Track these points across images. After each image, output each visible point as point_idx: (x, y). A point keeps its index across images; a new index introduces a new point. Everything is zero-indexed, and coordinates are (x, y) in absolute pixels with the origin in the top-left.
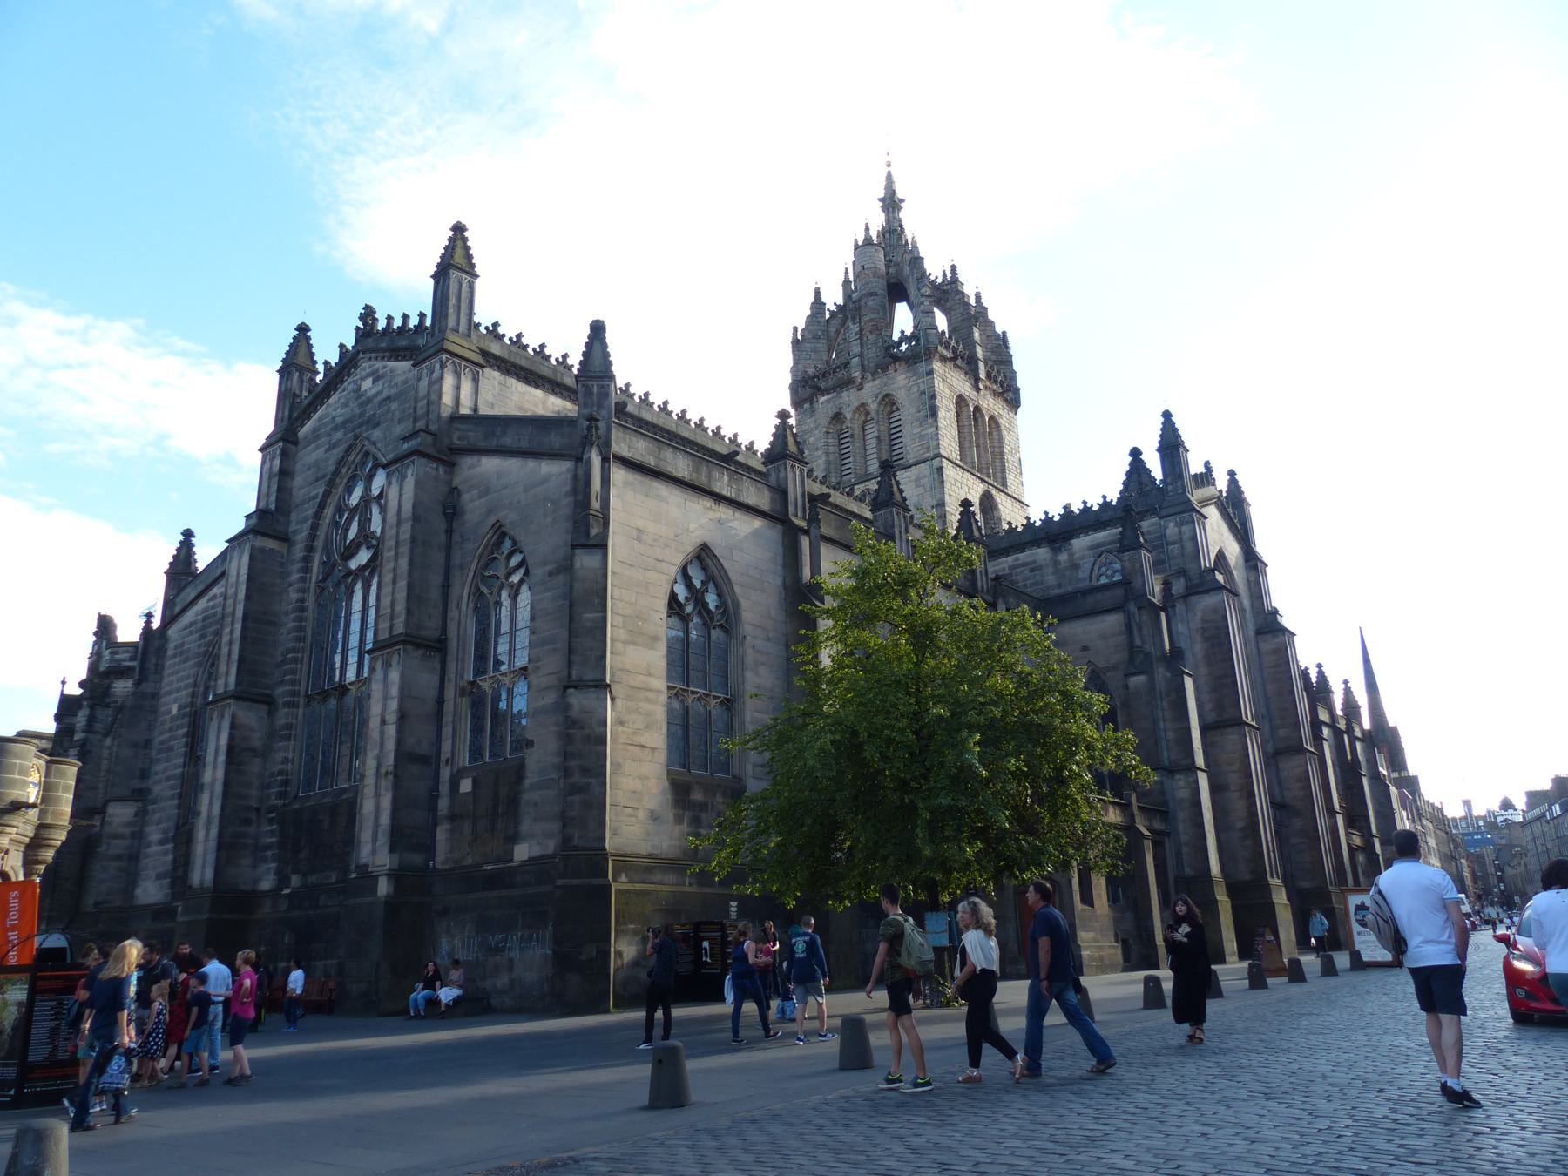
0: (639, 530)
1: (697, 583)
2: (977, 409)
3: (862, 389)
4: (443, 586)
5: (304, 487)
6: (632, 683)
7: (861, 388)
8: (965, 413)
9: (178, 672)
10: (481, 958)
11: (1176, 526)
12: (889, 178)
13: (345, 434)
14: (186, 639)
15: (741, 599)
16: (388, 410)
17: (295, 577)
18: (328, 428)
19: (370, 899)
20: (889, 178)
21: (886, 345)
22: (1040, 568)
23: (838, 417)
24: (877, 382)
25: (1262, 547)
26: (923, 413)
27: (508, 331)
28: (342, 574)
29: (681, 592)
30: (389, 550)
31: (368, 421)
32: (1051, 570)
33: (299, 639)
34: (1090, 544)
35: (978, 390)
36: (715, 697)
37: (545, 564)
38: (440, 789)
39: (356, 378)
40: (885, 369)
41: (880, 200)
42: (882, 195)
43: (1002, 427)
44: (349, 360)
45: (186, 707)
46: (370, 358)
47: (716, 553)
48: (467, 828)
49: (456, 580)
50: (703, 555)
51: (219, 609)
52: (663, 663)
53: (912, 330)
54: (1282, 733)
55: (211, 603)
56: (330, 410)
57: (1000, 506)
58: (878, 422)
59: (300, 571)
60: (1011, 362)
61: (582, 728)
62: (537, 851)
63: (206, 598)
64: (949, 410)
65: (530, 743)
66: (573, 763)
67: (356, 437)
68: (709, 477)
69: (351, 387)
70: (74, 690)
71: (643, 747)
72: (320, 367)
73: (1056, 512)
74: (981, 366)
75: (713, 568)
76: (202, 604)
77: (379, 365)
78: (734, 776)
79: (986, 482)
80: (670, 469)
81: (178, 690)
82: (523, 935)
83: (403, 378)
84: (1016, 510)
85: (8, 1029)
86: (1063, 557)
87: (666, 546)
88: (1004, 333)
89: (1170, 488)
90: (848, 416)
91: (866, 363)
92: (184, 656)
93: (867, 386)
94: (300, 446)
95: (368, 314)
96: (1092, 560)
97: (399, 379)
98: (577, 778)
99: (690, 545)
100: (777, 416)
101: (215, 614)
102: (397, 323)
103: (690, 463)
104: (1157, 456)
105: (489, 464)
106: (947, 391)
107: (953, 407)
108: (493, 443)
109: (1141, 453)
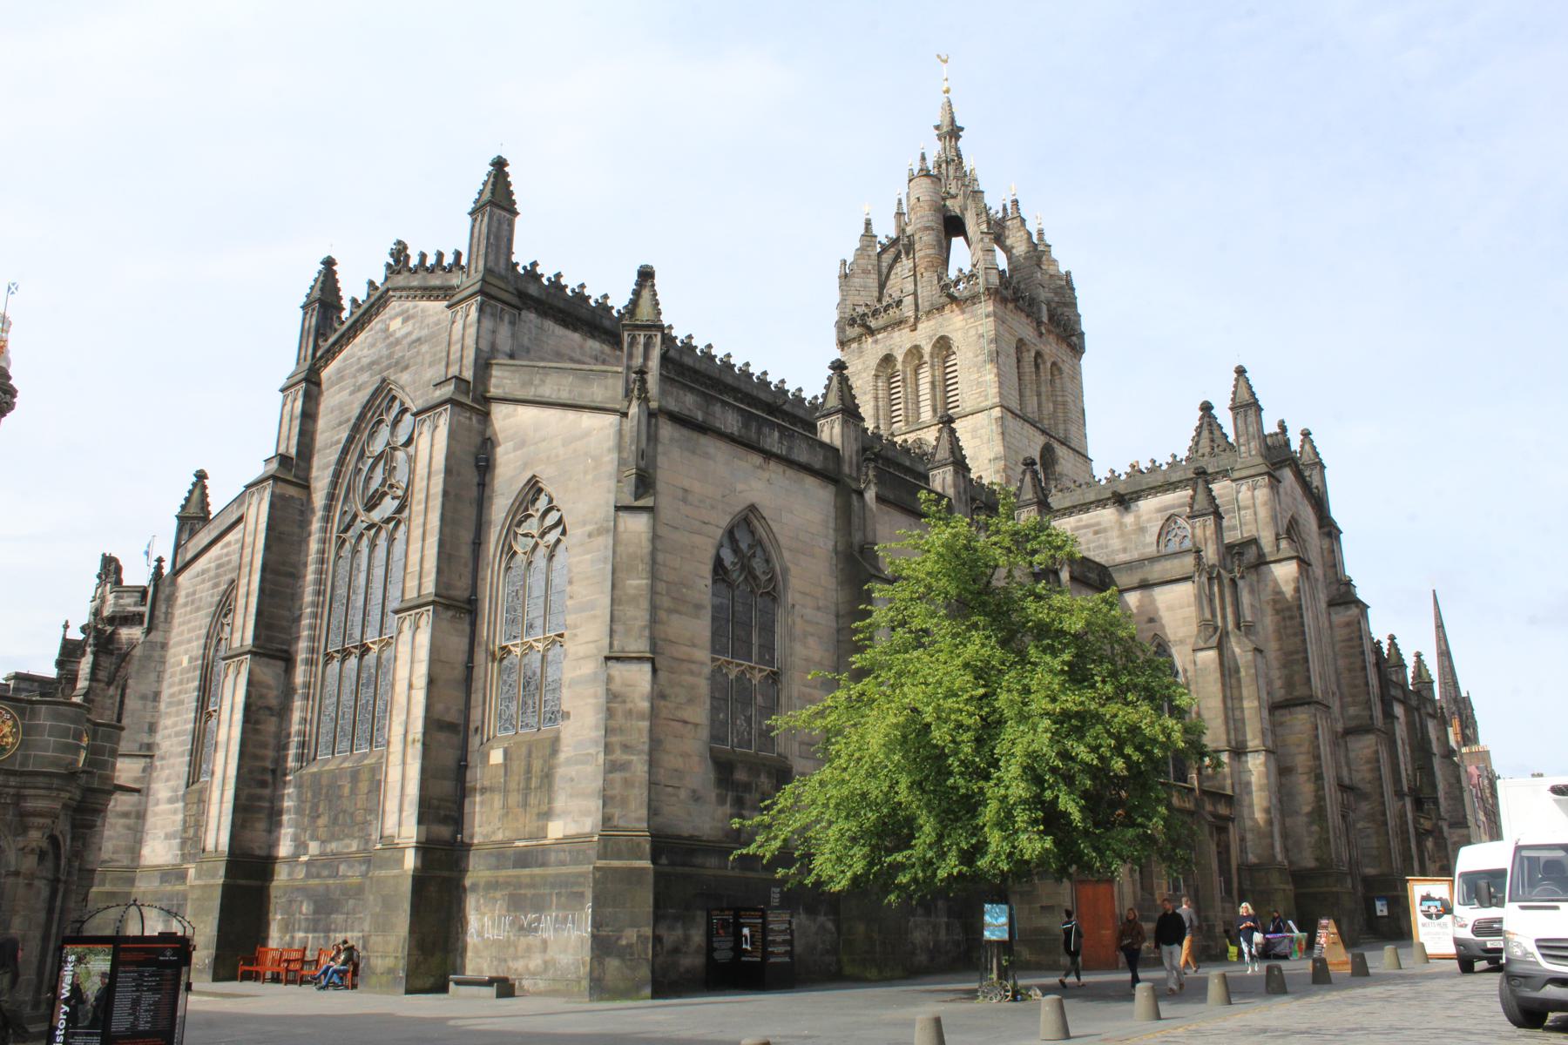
0: (686, 491)
1: (743, 546)
2: (1038, 354)
3: (915, 329)
4: (474, 543)
5: (330, 434)
6: (676, 654)
7: (914, 328)
8: (1026, 359)
9: (189, 621)
10: (512, 938)
11: (1249, 489)
13: (372, 376)
15: (789, 564)
16: (418, 353)
19: (395, 872)
21: (942, 283)
22: (1105, 530)
23: (888, 359)
24: (932, 323)
25: (1337, 512)
26: (981, 358)
27: (546, 271)
28: (365, 525)
29: (728, 557)
30: (419, 503)
31: (397, 363)
32: (1115, 533)
34: (1158, 506)
35: (1041, 335)
36: (761, 670)
37: (584, 524)
38: (469, 759)
40: (941, 309)
41: (937, 128)
43: (1065, 375)
44: (377, 301)
45: (197, 659)
46: (401, 297)
47: (764, 515)
48: (497, 801)
50: (749, 518)
51: (235, 557)
52: (707, 634)
53: (970, 268)
54: (1352, 711)
55: (225, 551)
57: (1061, 460)
58: (932, 366)
60: (1076, 304)
61: (624, 702)
62: (572, 829)
63: (220, 545)
64: (1008, 356)
65: (566, 715)
66: (614, 739)
67: (384, 380)
68: (759, 431)
69: (380, 326)
70: (76, 634)
71: (685, 722)
72: (346, 303)
73: (1123, 469)
74: (1044, 308)
75: (761, 532)
76: (216, 551)
77: (409, 304)
78: (779, 755)
79: (1047, 434)
80: (718, 425)
81: (189, 641)
82: (557, 916)
83: (435, 319)
84: (1079, 465)
85: (92, 999)
86: (1129, 519)
87: (713, 507)
88: (1068, 274)
89: (1243, 449)
90: (900, 359)
91: (920, 301)
92: (195, 605)
93: (920, 326)
94: (324, 386)
96: (1160, 523)
97: (431, 320)
98: (618, 755)
99: (739, 506)
100: (830, 368)
101: (229, 562)
102: (431, 260)
103: (740, 418)
104: (1230, 414)
105: (527, 415)
106: (1007, 335)
107: (1013, 351)
108: (530, 393)
109: (1212, 408)
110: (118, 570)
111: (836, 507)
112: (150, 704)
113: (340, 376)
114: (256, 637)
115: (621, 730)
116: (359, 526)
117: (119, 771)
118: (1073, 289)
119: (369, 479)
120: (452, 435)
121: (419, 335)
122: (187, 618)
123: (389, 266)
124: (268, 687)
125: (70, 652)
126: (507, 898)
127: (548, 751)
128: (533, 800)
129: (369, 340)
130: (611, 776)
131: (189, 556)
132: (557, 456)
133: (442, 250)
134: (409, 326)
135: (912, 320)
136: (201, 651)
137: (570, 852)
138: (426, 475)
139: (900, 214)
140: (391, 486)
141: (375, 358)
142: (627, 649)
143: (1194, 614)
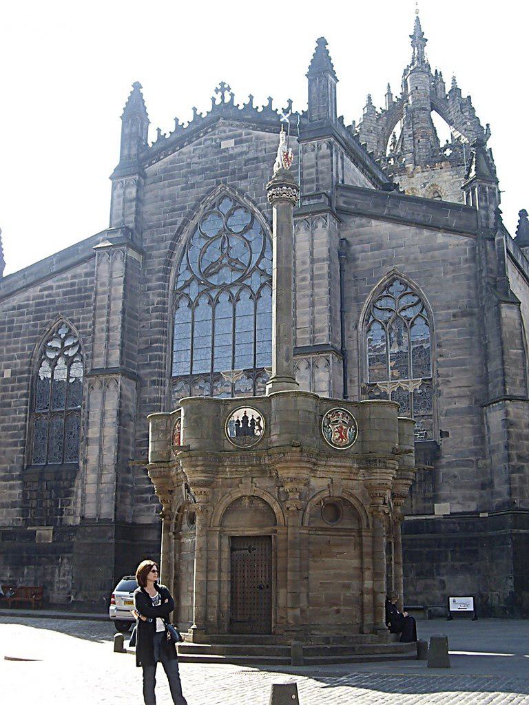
9: (8, 343)
12: (418, 20)
14: (15, 318)
20: (418, 20)
30: (304, 279)
31: (233, 172)
33: (164, 333)
37: (449, 308)
39: (213, 137)
42: (412, 34)
55: (46, 293)
56: (185, 157)
59: (159, 279)
62: (458, 509)
63: (39, 288)
76: (35, 291)
91: (417, 158)
95: (223, 88)
97: (268, 146)
98: (515, 462)
101: (53, 302)
102: (260, 103)
113: (168, 174)
114: (122, 363)
115: (517, 448)
120: (330, 234)
121: (256, 155)
123: (214, 99)
124: (129, 400)
129: (198, 152)
130: (514, 475)
132: (416, 259)
134: (244, 147)
135: (411, 170)
137: (459, 523)
138: (309, 261)
140: (231, 261)
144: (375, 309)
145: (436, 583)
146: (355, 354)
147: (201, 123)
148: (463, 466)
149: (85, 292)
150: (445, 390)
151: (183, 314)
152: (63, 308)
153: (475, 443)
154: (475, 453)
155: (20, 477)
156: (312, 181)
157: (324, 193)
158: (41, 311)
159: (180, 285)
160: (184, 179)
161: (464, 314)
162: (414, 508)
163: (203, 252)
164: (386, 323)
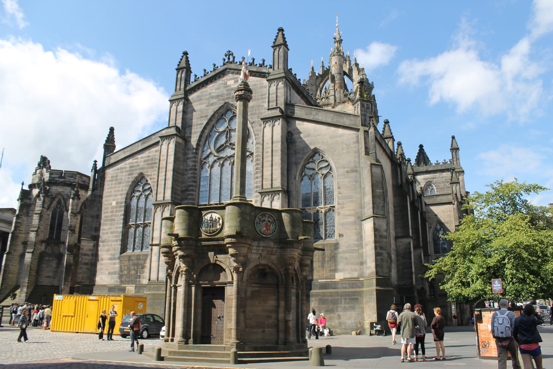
9: (115, 188)
13: (218, 101)
14: (119, 174)
17: (190, 155)
18: (208, 97)
21: (345, 93)
28: (216, 158)
30: (267, 152)
33: (195, 182)
37: (344, 168)
49: (294, 168)
62: (348, 276)
65: (341, 235)
70: (26, 188)
76: (130, 161)
81: (116, 196)
83: (254, 83)
89: (454, 162)
95: (229, 54)
96: (424, 184)
98: (378, 250)
110: (49, 162)
111: (392, 170)
112: (95, 220)
114: (172, 197)
116: (211, 159)
117: (83, 246)
118: (375, 101)
119: (217, 139)
122: (113, 186)
123: (224, 60)
125: (25, 195)
126: (318, 300)
127: (333, 248)
128: (326, 265)
131: (112, 161)
133: (254, 58)
136: (124, 200)
137: (348, 284)
139: (323, 67)
140: (231, 144)
141: (220, 94)
142: (378, 214)
143: (453, 215)
144: (306, 169)
145: (336, 316)
146: (294, 193)
147: (217, 72)
148: (351, 252)
149: (155, 160)
150: (342, 212)
151: (205, 173)
152: (143, 168)
153: (357, 240)
154: (358, 246)
155: (119, 258)
156: (273, 101)
157: (279, 107)
158: (131, 170)
159: (204, 156)
160: (207, 101)
161: (352, 171)
162: (324, 275)
163: (217, 139)
164: (311, 176)
